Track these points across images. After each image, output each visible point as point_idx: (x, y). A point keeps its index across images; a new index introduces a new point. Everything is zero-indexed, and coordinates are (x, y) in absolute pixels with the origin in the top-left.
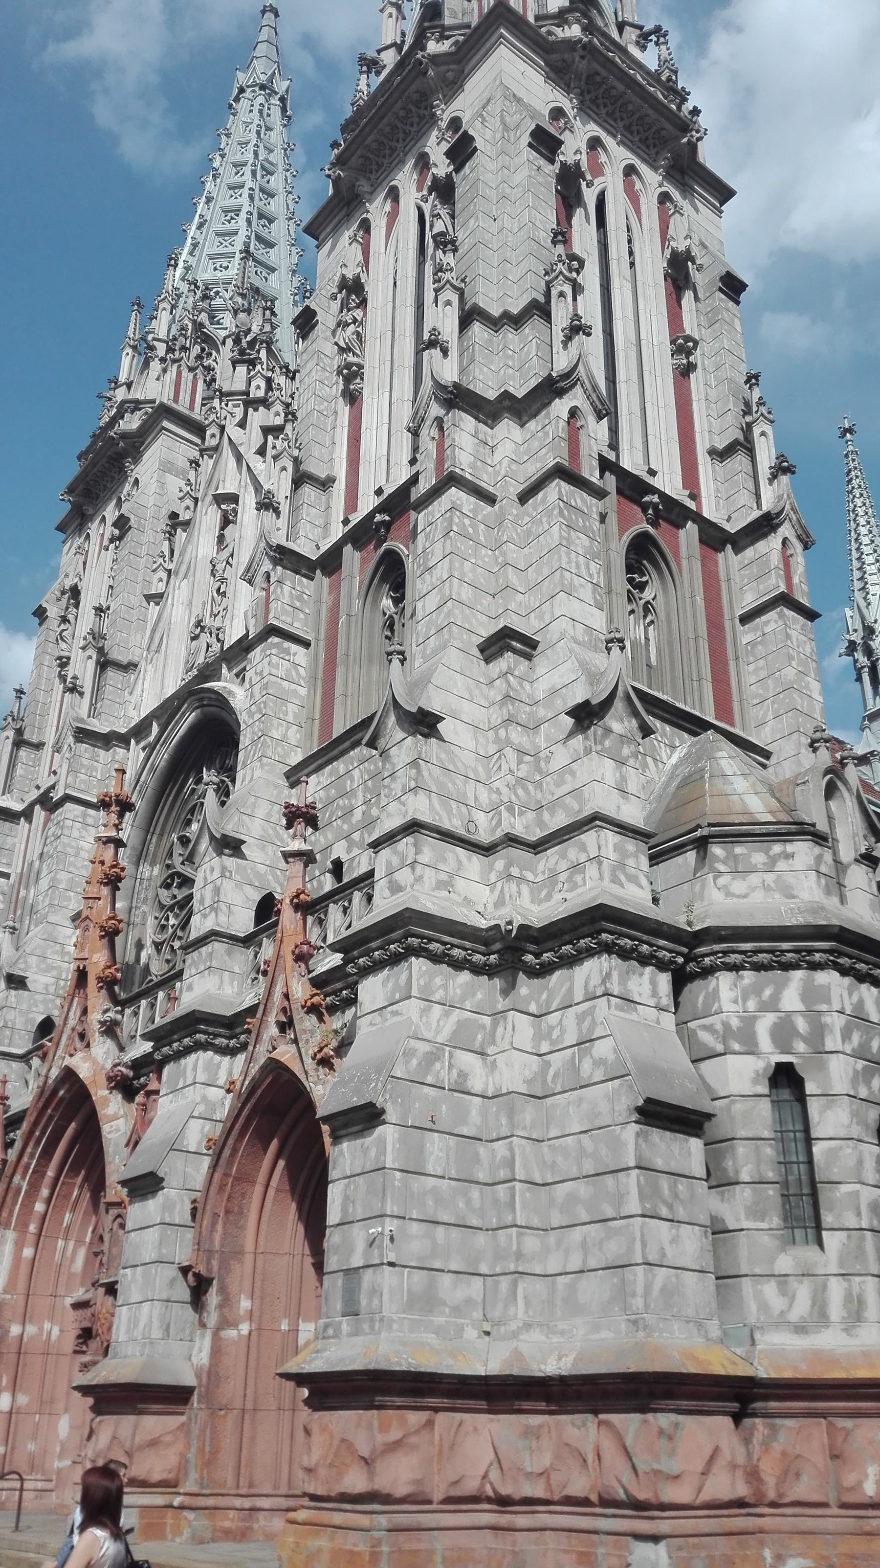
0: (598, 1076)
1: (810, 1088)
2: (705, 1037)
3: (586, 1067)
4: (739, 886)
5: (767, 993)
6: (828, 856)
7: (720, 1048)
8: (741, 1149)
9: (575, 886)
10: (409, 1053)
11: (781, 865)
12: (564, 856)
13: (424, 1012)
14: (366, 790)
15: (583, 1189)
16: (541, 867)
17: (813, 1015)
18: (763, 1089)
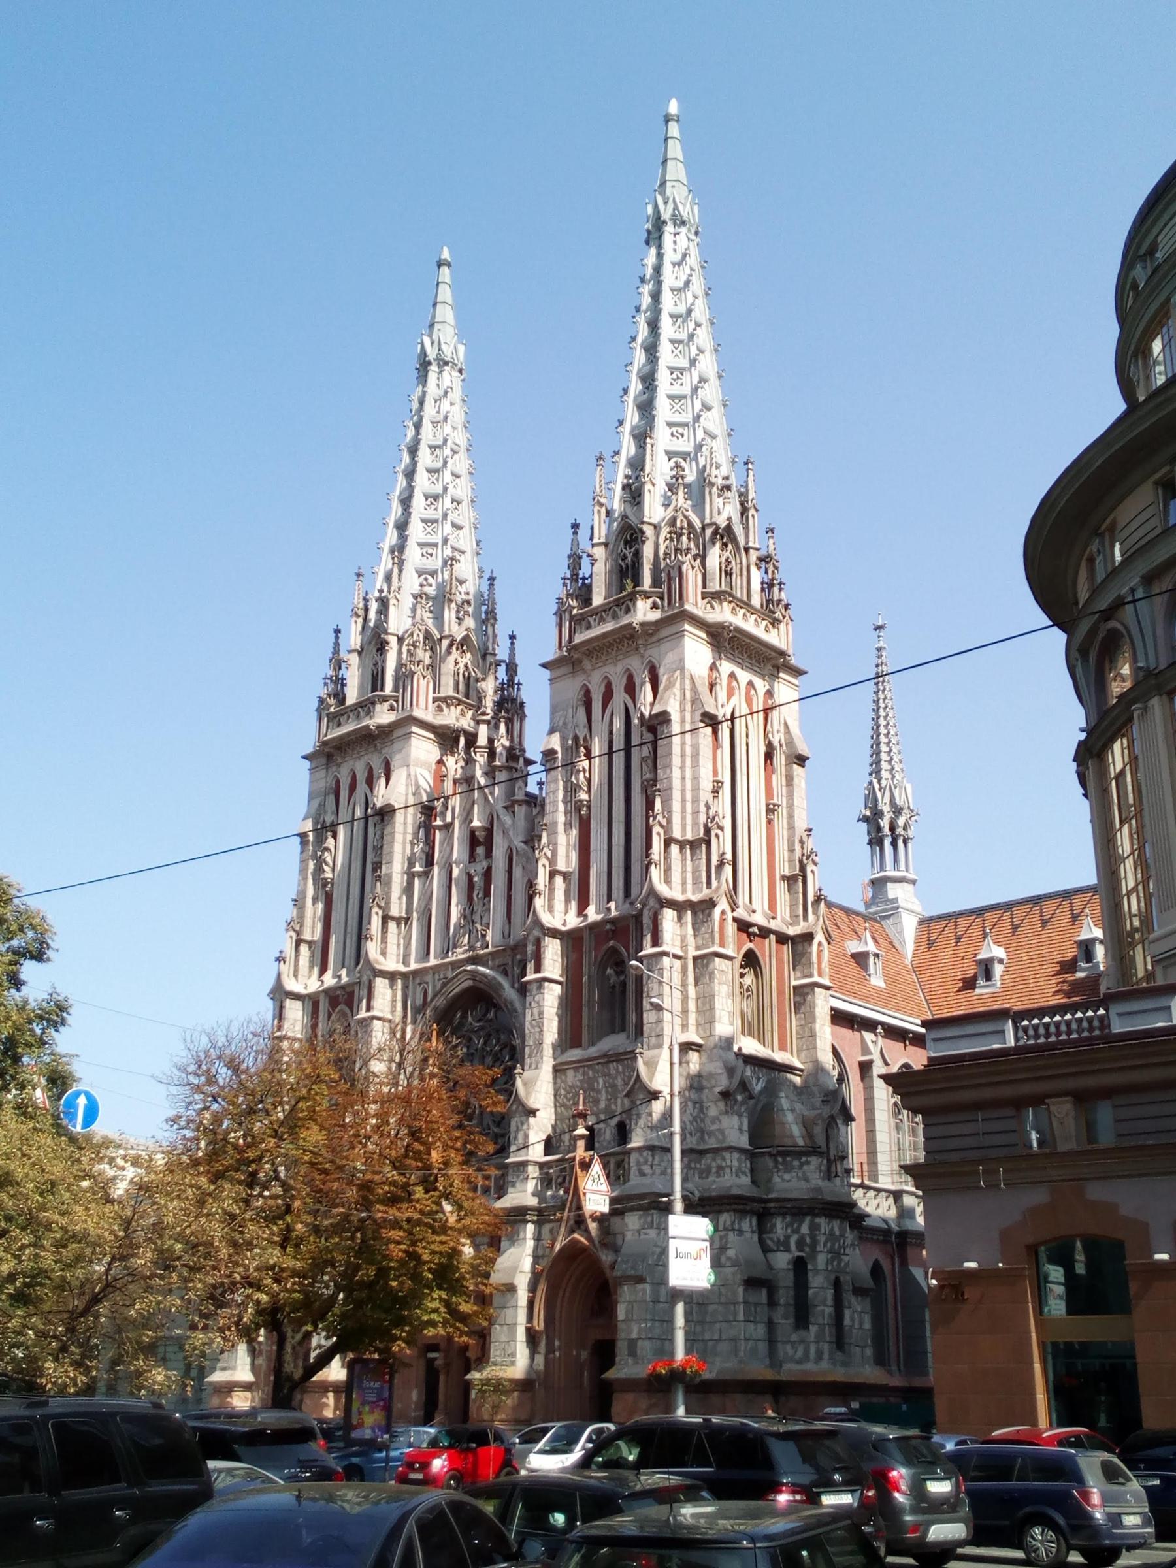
0: (728, 1264)
1: (810, 1267)
2: (770, 1243)
3: (723, 1259)
4: (787, 1176)
5: (795, 1225)
6: (825, 1161)
7: (775, 1248)
8: (781, 1292)
9: (718, 1176)
10: (653, 1254)
11: (805, 1167)
12: (714, 1160)
13: (658, 1234)
14: (607, 1092)
15: (721, 1308)
16: (703, 1162)
17: (813, 1237)
18: (790, 1267)
